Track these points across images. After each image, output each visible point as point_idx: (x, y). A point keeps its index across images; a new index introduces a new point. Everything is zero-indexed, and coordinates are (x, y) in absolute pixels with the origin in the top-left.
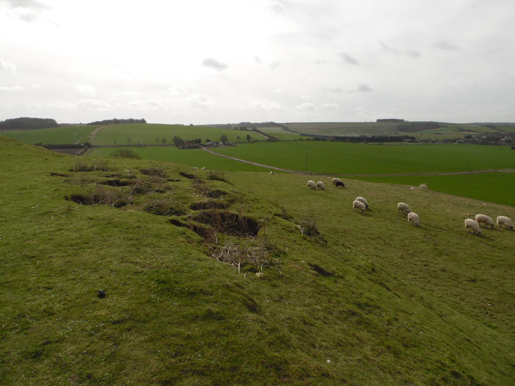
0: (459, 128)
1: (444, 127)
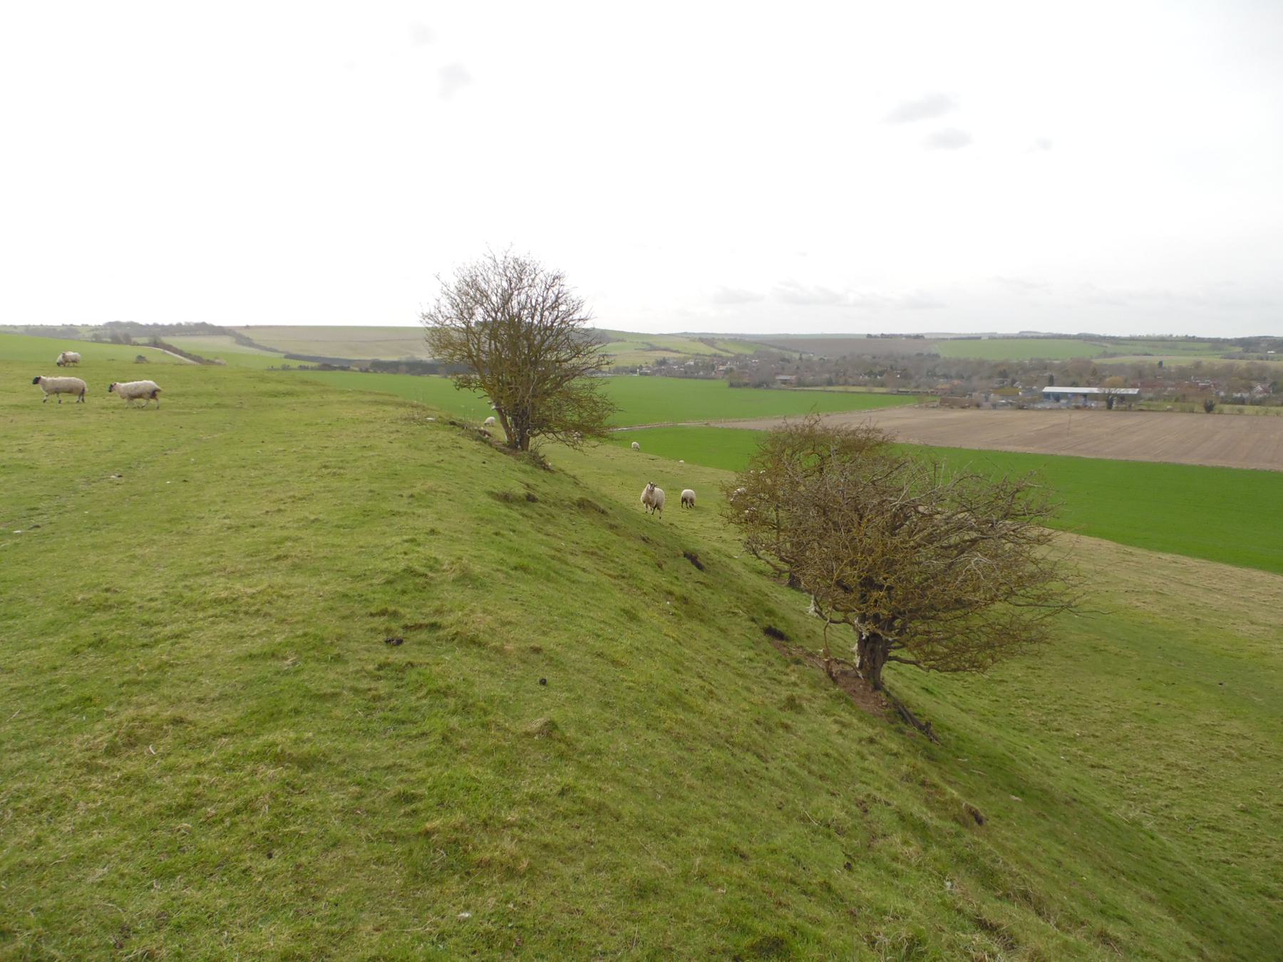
0: (648, 343)
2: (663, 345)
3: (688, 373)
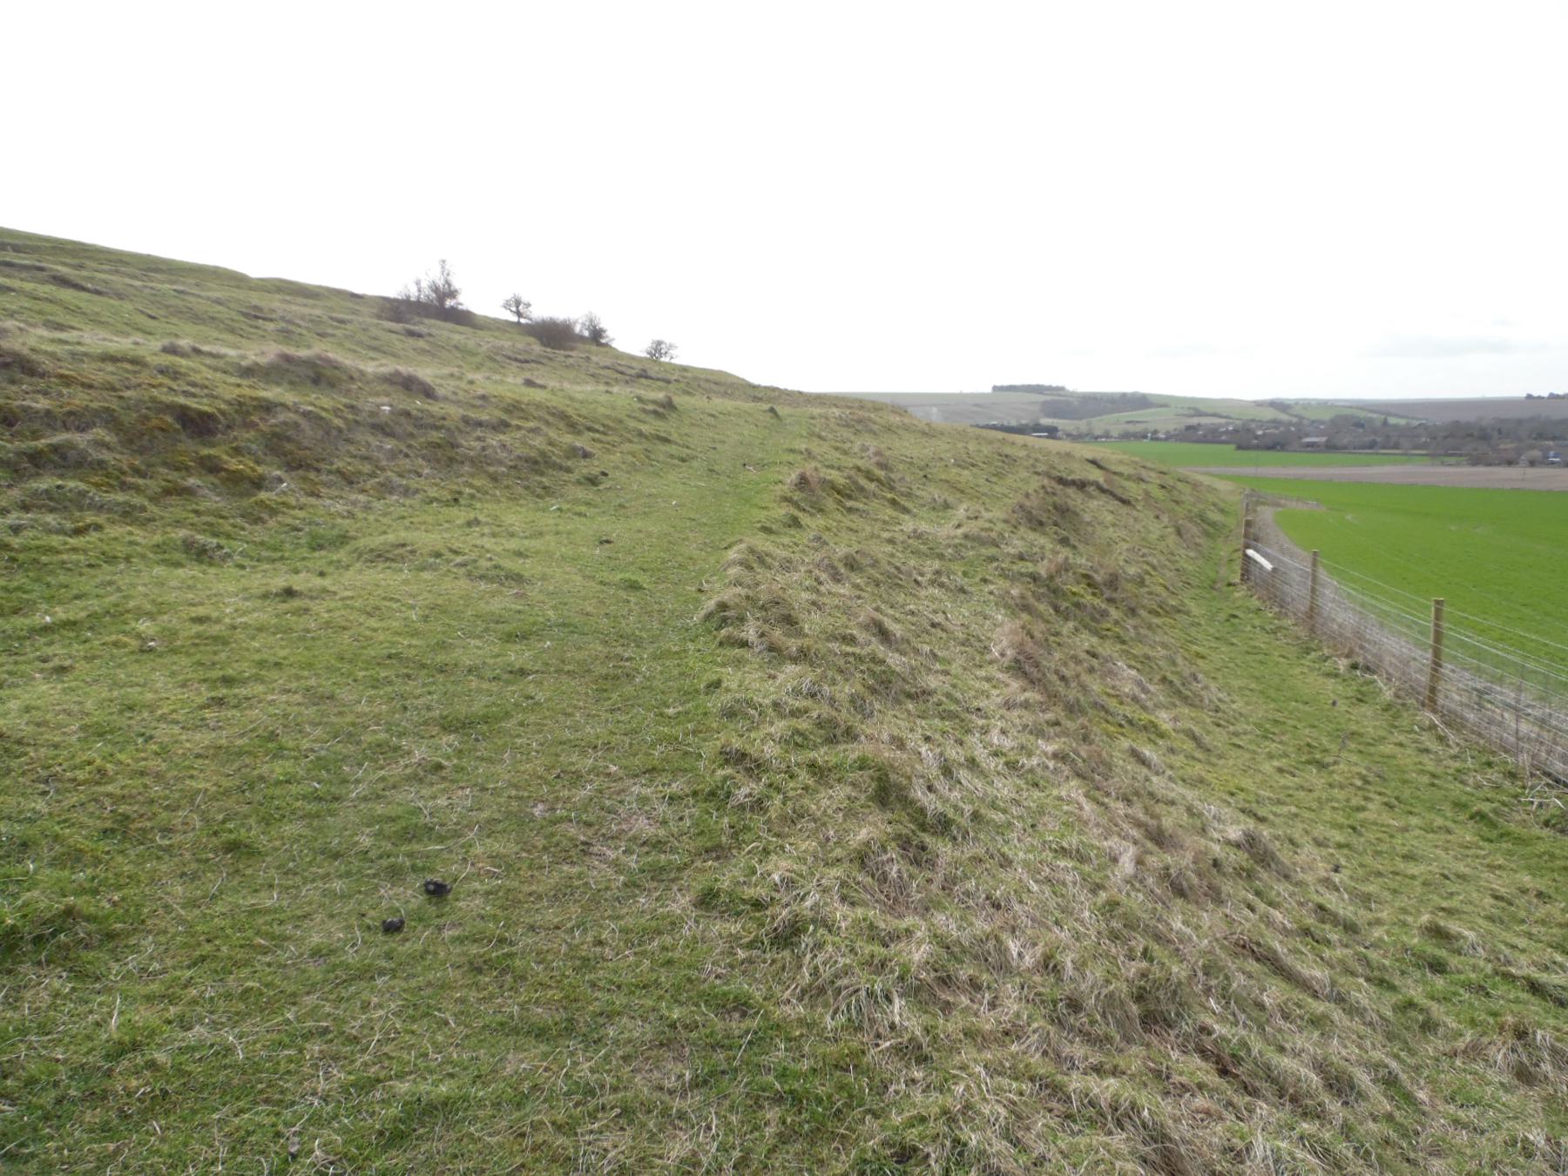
0: (1195, 408)
1: (1162, 406)
2: (1210, 411)
3: (1212, 436)
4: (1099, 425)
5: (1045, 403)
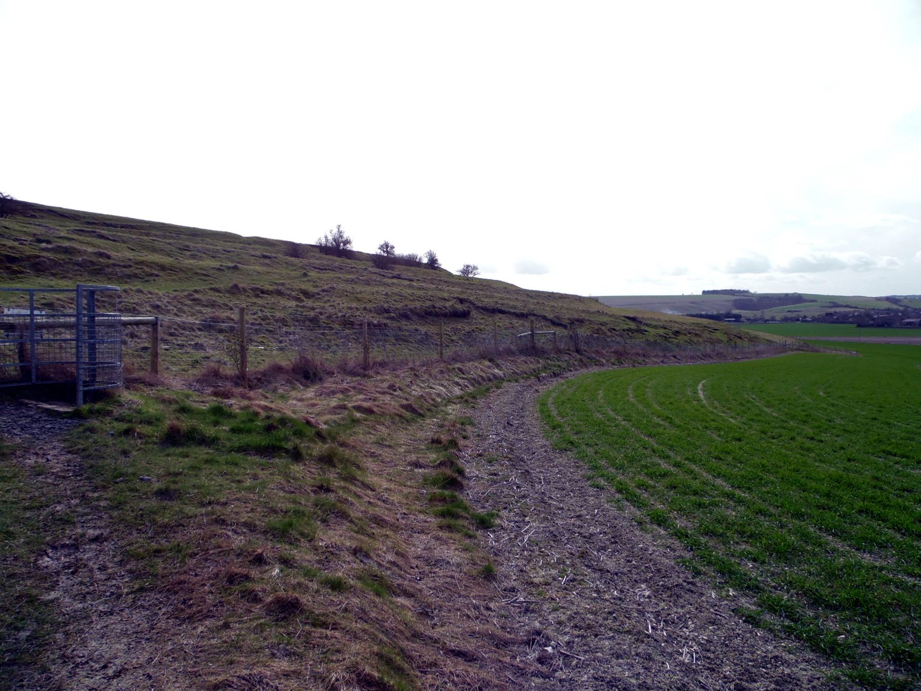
0: (834, 302)
1: (812, 301)
2: (844, 304)
3: (843, 319)
4: (768, 314)
5: (735, 301)
